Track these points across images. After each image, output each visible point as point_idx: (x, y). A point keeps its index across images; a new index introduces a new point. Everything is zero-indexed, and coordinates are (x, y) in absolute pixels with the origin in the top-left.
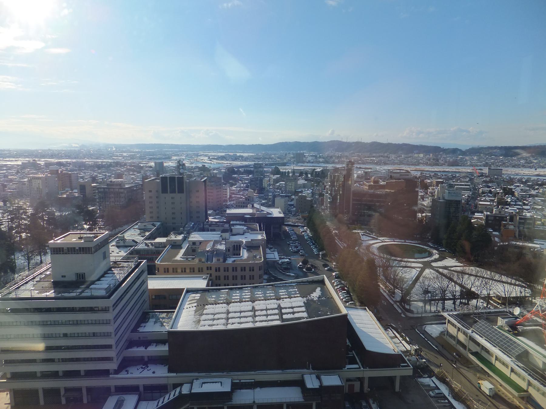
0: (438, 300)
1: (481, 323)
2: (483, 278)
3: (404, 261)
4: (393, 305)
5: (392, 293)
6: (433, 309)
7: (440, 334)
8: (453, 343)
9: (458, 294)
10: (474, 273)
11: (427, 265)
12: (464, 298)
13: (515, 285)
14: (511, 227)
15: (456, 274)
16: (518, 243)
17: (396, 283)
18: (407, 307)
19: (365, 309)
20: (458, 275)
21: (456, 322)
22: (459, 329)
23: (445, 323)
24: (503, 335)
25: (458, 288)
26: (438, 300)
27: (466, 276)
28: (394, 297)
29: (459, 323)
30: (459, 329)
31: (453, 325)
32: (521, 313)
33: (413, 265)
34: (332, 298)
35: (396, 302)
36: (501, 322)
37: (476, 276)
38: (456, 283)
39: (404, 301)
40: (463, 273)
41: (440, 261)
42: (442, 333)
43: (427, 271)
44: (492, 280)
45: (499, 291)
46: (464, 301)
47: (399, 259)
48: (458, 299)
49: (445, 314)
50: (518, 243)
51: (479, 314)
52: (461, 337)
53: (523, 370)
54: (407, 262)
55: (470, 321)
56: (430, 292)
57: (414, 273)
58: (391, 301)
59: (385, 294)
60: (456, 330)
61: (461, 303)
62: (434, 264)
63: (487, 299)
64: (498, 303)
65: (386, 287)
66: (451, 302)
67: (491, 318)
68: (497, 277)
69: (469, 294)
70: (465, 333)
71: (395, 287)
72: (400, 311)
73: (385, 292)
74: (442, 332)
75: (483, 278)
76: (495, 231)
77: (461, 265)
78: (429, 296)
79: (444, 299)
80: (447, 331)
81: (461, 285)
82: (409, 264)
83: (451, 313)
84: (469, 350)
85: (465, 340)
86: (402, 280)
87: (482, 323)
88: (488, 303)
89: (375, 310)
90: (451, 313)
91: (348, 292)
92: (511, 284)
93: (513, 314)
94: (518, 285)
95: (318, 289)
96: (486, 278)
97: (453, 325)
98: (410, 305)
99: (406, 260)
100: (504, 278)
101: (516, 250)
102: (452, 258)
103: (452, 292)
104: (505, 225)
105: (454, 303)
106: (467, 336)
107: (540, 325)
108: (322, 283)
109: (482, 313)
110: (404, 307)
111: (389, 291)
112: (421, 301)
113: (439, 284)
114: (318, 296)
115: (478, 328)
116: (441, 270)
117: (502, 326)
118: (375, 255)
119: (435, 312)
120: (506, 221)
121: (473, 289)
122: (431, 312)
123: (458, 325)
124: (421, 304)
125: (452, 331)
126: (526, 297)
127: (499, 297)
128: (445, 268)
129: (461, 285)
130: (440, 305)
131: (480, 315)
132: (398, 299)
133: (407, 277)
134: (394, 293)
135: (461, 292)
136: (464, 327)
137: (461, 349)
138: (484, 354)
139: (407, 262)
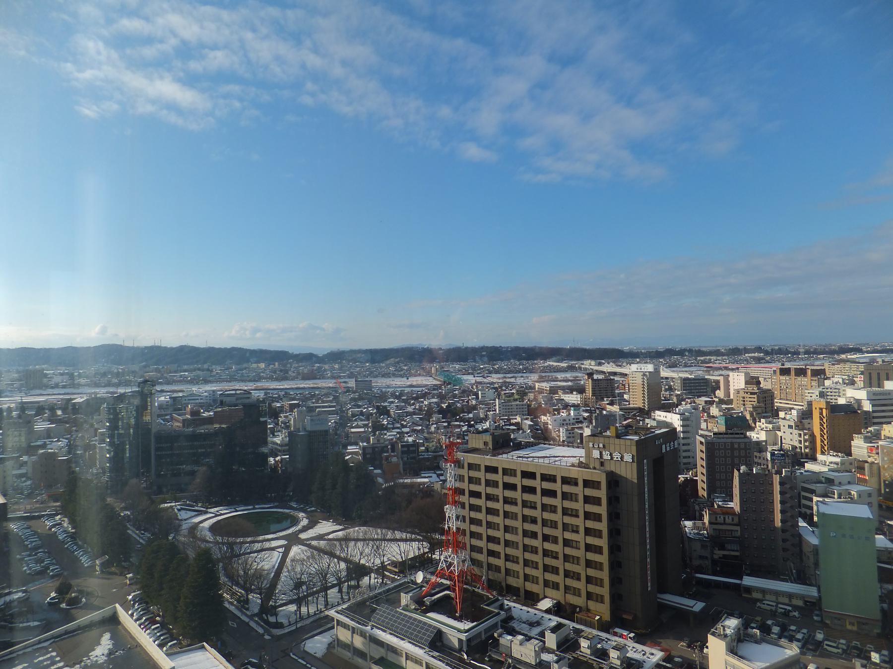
0: (317, 592)
1: (380, 610)
2: (373, 540)
3: (259, 542)
4: (247, 624)
5: (244, 603)
6: (312, 610)
7: (328, 649)
8: (347, 655)
9: (344, 574)
10: (361, 536)
11: (293, 540)
12: (352, 579)
13: (412, 540)
14: (394, 459)
15: (337, 543)
16: (406, 481)
17: (249, 581)
18: (272, 619)
19: (203, 647)
20: (341, 545)
21: (348, 620)
22: (354, 631)
23: (333, 628)
24: (410, 618)
25: (343, 565)
26: (317, 592)
27: (352, 544)
28: (247, 609)
29: (352, 620)
30: (354, 631)
31: (345, 626)
32: (424, 578)
33: (274, 544)
34: (139, 645)
35: (251, 617)
36: (405, 599)
37: (364, 540)
38: (339, 558)
39: (267, 610)
40: (346, 539)
41: (311, 528)
42: (330, 646)
43: (296, 551)
44: (385, 540)
45: (394, 554)
46: (353, 583)
47: (249, 539)
48: (345, 582)
49: (332, 613)
50: (406, 481)
51: (376, 597)
52: (358, 642)
53: (440, 660)
54: (262, 541)
55: (367, 611)
56: (304, 583)
57: (276, 556)
58: (244, 618)
59: (232, 608)
60: (350, 633)
61: (349, 587)
62: (303, 536)
63: (381, 570)
64: (395, 573)
65: (233, 594)
66: (336, 590)
67: (390, 597)
68: (389, 535)
69: (358, 571)
70: (363, 634)
71: (248, 591)
72: (261, 631)
73: (231, 603)
74: (329, 645)
75: (373, 540)
76: (375, 469)
77: (341, 527)
78: (303, 592)
79: (325, 589)
80: (338, 640)
81: (346, 560)
82: (267, 545)
83: (340, 608)
84: (372, 658)
85: (364, 644)
86: (259, 575)
87: (383, 610)
88: (384, 576)
89: (219, 643)
90: (340, 608)
91: (163, 626)
92: (406, 540)
93: (415, 583)
94: (414, 540)
95: (107, 636)
96: (377, 540)
97: (345, 626)
98: (276, 615)
99: (261, 538)
100: (398, 535)
101: (406, 491)
102: (327, 519)
103: (336, 573)
104: (387, 458)
105: (340, 591)
106: (365, 637)
107: (448, 588)
108: (113, 621)
109: (380, 594)
110: (267, 622)
111: (239, 601)
112: (291, 602)
113: (316, 566)
114: (106, 652)
115: (379, 619)
116: (314, 543)
117: (407, 605)
118: (207, 542)
119: (315, 614)
120: (387, 452)
121: (363, 562)
122: (309, 616)
123: (352, 624)
124: (292, 608)
125: (344, 635)
126: (424, 553)
127: (394, 564)
128: (320, 537)
129: (346, 560)
130: (321, 600)
131: (377, 599)
132: (256, 610)
133: (266, 567)
134: (247, 601)
135: (348, 568)
136: (360, 624)
137: (360, 660)
138: (391, 657)
139: (262, 541)
